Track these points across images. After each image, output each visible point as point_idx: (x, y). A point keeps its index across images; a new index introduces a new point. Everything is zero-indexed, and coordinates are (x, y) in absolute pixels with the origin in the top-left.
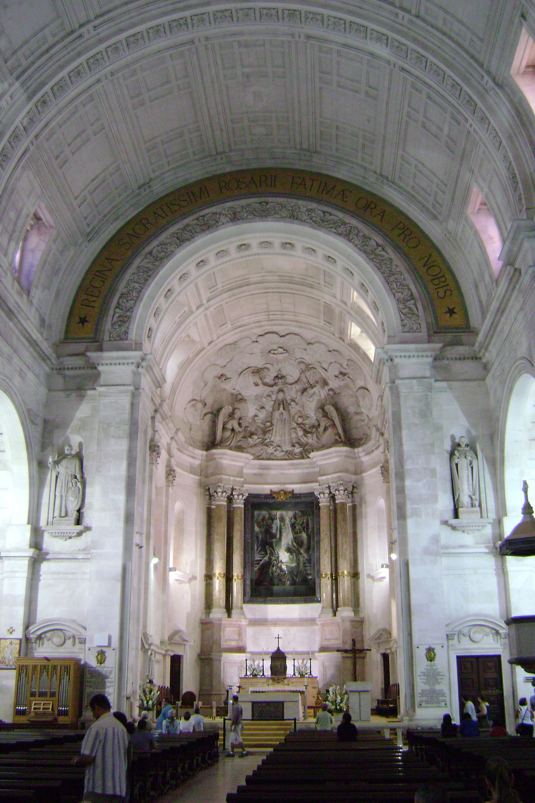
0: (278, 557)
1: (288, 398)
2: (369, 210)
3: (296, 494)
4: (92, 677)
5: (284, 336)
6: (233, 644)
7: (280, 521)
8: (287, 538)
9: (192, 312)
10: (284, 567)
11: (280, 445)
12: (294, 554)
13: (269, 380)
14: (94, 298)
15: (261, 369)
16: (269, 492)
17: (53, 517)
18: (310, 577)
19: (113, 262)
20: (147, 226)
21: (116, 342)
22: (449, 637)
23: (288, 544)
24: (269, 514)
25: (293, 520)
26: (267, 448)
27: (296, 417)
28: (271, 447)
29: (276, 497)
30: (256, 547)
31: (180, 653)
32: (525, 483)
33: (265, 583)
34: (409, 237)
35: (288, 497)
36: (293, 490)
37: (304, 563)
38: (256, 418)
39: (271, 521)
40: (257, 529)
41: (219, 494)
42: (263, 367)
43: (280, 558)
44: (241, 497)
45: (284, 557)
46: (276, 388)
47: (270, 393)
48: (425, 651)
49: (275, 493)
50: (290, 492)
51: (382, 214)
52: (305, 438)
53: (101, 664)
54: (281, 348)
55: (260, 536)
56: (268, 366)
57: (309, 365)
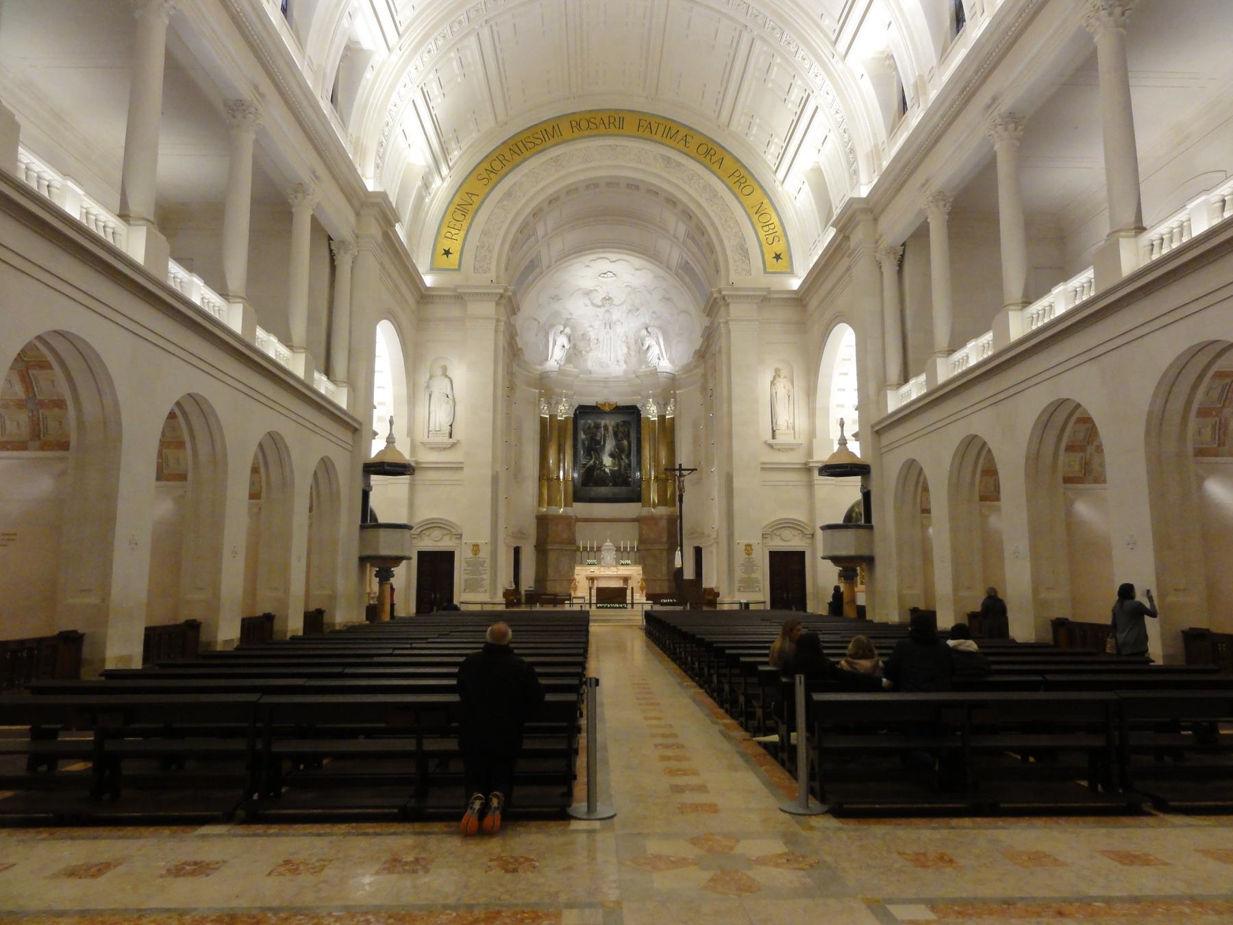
0: (602, 462)
2: (709, 157)
3: (619, 407)
4: (468, 566)
5: (614, 262)
6: (565, 536)
7: (604, 430)
8: (610, 445)
9: (538, 241)
10: (607, 470)
12: (617, 460)
13: (598, 301)
14: (457, 232)
15: (591, 291)
16: (594, 405)
17: (429, 431)
18: (630, 480)
19: (473, 197)
20: (504, 162)
21: (478, 274)
22: (764, 536)
23: (611, 451)
24: (595, 423)
25: (615, 429)
29: (602, 408)
30: (582, 452)
31: (519, 545)
32: (842, 419)
33: (591, 484)
34: (745, 185)
37: (625, 467)
39: (595, 430)
40: (583, 436)
43: (604, 463)
45: (607, 461)
46: (603, 309)
48: (744, 547)
49: (600, 404)
50: (613, 405)
51: (720, 161)
53: (476, 555)
54: (611, 272)
55: (586, 443)
57: (635, 288)
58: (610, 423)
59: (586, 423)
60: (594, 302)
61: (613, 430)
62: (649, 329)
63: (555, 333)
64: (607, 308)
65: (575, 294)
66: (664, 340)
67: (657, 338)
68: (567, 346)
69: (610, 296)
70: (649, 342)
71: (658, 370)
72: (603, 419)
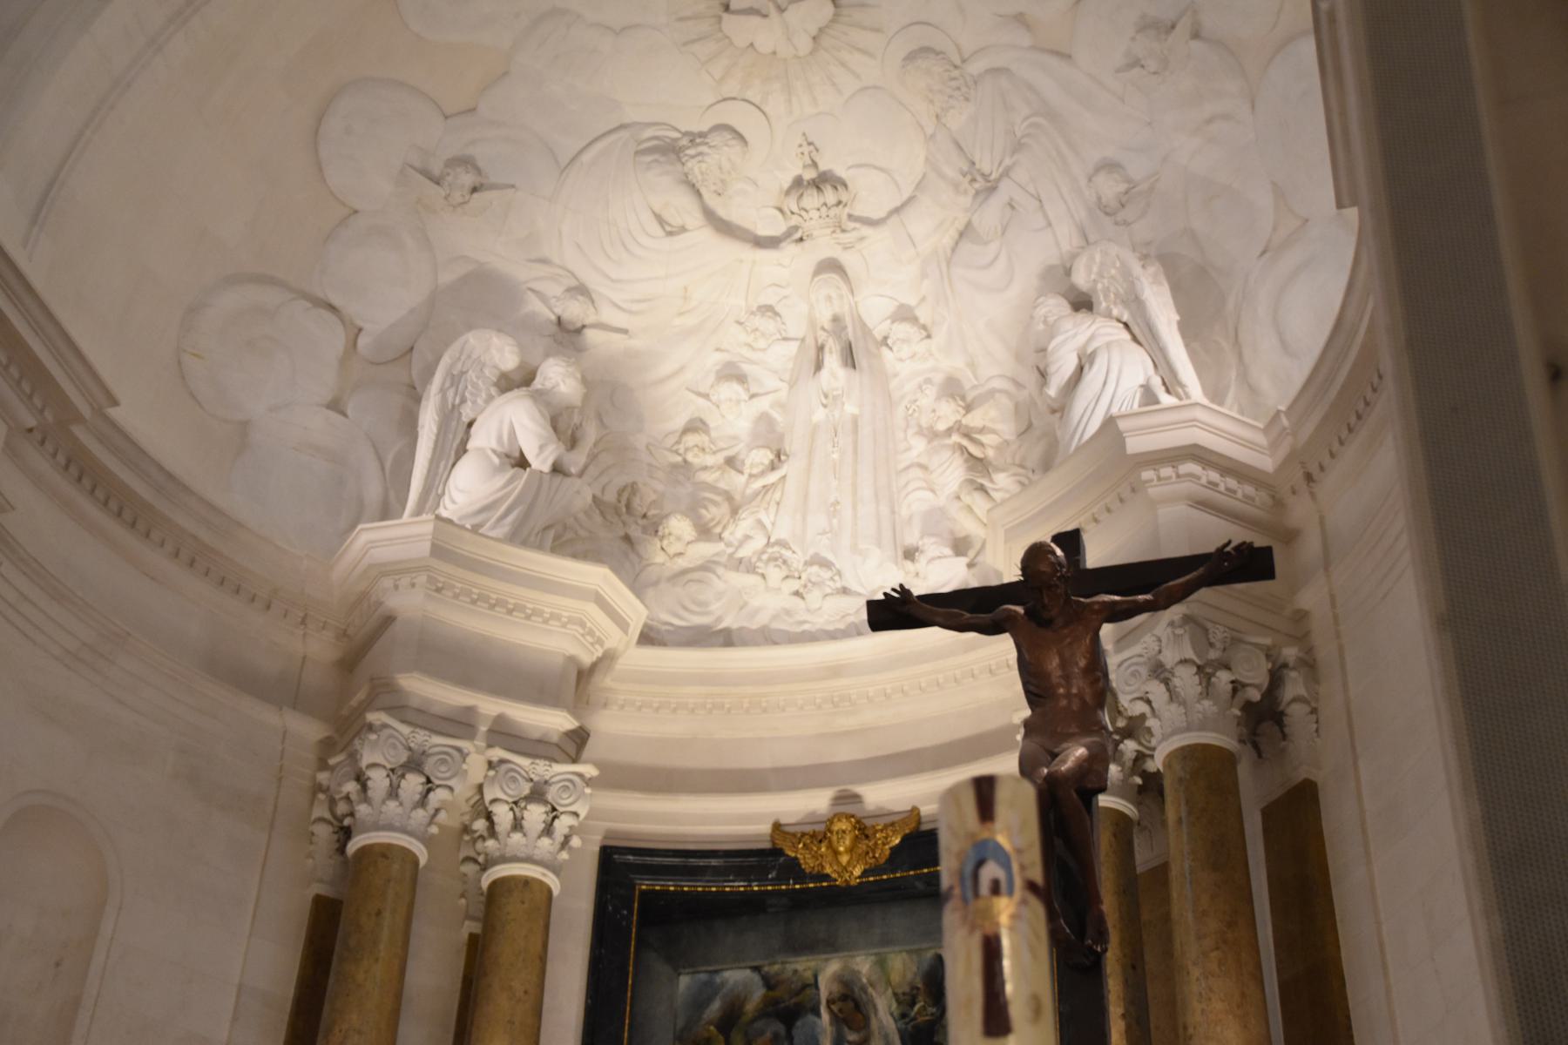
1: (874, 307)
7: (836, 1019)
11: (830, 557)
15: (695, 138)
24: (769, 983)
26: (751, 580)
27: (927, 399)
28: (775, 574)
29: (808, 863)
35: (883, 853)
36: (915, 811)
38: (691, 439)
41: (379, 781)
42: (705, 128)
44: (535, 815)
47: (769, 298)
52: (979, 503)
56: (736, 116)
58: (881, 963)
59: (699, 1002)
60: (736, 211)
61: (903, 1016)
62: (1081, 279)
63: (455, 379)
64: (824, 245)
65: (587, 157)
66: (1180, 308)
67: (1135, 301)
68: (540, 462)
69: (823, 167)
70: (1081, 339)
71: (1135, 445)
72: (830, 946)
